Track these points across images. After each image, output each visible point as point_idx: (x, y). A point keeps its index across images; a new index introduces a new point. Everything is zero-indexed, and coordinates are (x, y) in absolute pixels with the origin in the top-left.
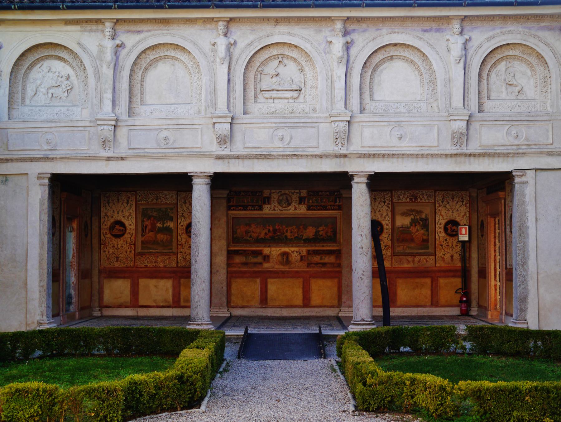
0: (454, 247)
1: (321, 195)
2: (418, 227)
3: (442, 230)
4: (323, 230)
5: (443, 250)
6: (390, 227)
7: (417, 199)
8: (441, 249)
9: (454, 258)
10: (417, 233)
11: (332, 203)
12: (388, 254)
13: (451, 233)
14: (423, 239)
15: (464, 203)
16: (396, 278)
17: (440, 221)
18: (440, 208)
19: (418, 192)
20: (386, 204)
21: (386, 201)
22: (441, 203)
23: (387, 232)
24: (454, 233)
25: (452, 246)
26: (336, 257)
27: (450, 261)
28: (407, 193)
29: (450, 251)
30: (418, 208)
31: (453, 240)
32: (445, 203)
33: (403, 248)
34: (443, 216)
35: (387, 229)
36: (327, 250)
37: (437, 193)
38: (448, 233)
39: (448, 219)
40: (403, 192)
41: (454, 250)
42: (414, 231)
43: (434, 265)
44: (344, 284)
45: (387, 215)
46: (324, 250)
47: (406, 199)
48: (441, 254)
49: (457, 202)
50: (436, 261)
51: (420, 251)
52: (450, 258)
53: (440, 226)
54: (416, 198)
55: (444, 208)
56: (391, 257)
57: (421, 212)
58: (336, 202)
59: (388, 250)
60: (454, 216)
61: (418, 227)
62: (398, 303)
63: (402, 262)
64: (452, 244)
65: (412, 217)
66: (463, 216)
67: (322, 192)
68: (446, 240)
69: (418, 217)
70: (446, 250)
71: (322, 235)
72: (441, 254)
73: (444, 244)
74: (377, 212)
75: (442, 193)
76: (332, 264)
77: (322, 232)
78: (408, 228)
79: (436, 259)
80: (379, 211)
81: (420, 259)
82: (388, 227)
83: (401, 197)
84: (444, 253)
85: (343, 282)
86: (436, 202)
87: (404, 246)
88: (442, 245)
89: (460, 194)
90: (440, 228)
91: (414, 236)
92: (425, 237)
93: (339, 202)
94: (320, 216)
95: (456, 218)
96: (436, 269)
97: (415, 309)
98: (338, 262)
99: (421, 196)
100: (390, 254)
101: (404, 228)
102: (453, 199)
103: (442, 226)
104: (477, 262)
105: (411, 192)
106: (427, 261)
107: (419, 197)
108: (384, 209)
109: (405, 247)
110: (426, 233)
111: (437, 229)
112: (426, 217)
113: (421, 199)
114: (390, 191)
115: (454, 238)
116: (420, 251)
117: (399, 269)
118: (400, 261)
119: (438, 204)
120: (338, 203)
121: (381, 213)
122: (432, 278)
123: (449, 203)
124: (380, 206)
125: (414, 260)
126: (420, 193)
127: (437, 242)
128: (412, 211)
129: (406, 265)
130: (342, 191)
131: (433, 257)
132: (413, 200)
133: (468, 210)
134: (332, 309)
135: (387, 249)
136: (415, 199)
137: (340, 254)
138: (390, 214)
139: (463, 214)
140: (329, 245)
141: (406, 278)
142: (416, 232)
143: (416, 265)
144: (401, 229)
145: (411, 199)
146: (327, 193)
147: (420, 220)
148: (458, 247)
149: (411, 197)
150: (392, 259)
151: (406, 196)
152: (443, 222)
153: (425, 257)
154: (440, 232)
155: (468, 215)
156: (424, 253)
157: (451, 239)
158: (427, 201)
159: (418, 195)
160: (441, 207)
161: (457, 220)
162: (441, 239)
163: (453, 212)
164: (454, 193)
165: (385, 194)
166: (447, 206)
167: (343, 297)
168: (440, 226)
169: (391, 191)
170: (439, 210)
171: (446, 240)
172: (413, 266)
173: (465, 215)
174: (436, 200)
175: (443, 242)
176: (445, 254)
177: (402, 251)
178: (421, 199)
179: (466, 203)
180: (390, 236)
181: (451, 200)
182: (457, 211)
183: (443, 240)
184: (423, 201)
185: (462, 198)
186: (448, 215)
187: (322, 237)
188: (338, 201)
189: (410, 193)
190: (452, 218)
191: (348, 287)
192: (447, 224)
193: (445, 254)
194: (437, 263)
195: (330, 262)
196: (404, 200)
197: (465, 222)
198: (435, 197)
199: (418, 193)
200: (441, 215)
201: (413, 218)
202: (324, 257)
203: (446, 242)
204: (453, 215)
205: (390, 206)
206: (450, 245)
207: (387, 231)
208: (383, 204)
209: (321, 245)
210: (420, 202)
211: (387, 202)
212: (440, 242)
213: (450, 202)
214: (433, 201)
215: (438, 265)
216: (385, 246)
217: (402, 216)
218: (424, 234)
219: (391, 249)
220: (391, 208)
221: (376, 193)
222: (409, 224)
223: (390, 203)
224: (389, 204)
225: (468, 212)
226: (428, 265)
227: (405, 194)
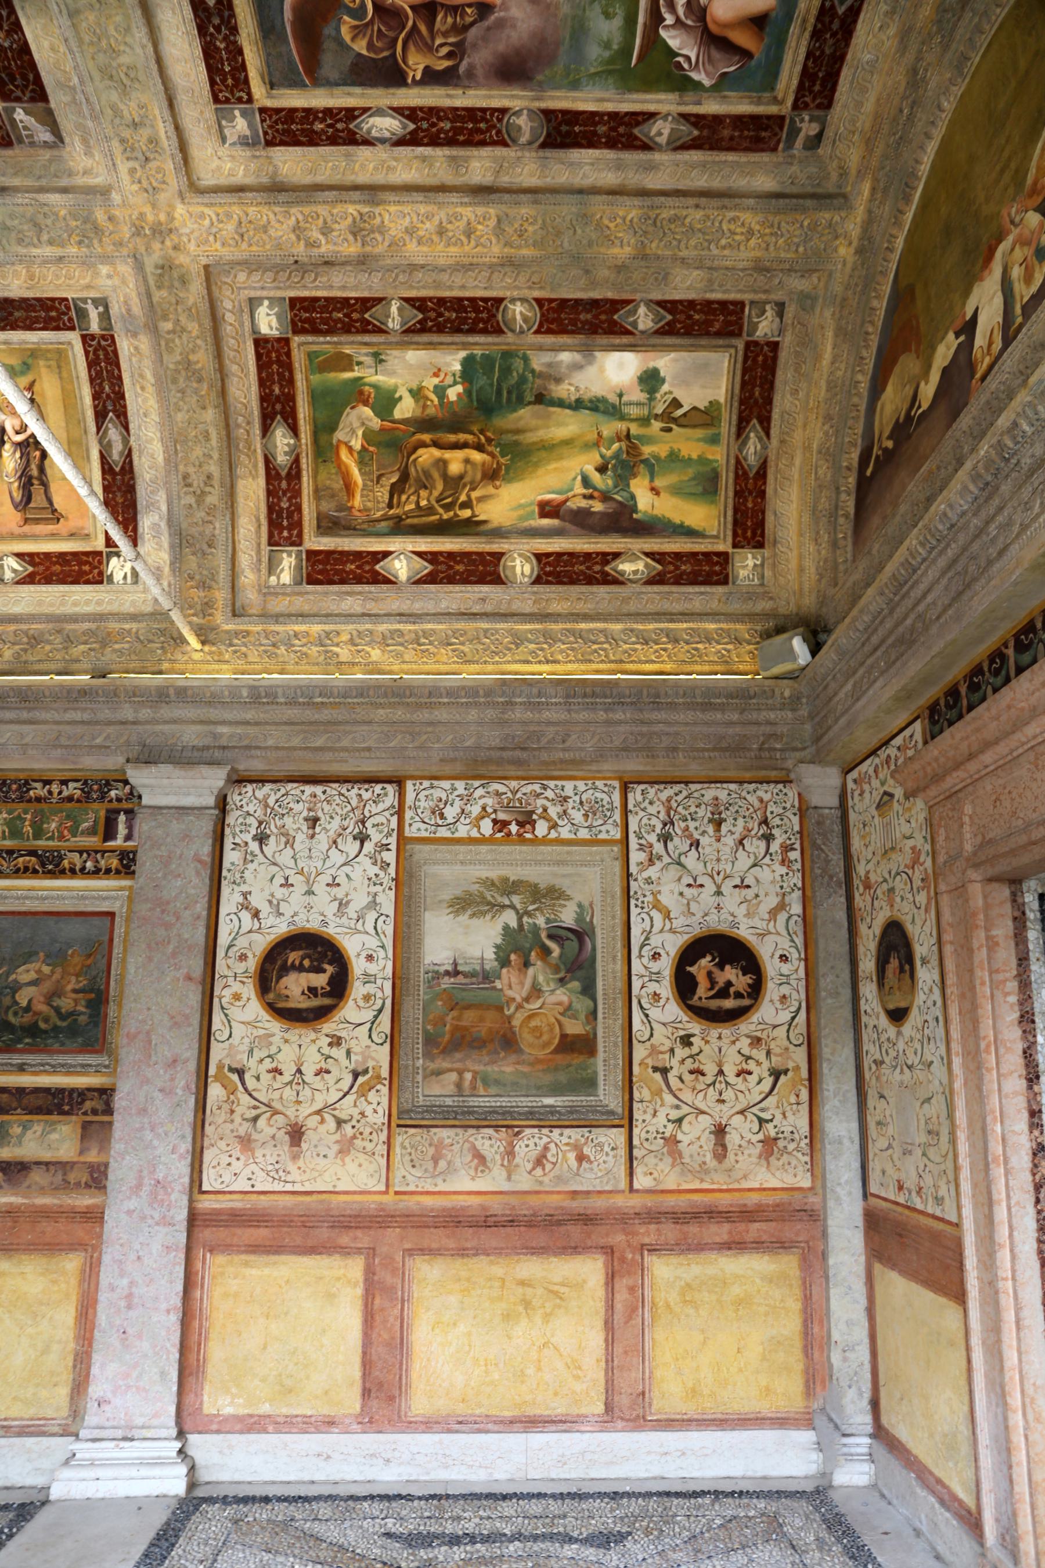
0: (732, 1079)
1: (38, 799)
2: (538, 971)
3: (666, 988)
4: (34, 983)
5: (669, 1098)
6: (384, 967)
7: (533, 823)
8: (658, 1093)
9: (732, 1139)
10: (538, 1004)
11: (93, 841)
12: (372, 1118)
13: (714, 1004)
14: (564, 1036)
15: (775, 847)
16: (410, 1252)
17: (655, 941)
18: (652, 872)
19: (537, 787)
20: (369, 846)
21: (371, 831)
22: (658, 848)
23: (367, 998)
24: (729, 1004)
25: (721, 1072)
26: (86, 1126)
27: (709, 1157)
28: (480, 792)
29: (706, 1101)
30: (538, 875)
31: (725, 1043)
32: (679, 844)
33: (459, 1085)
34: (667, 915)
35: (369, 978)
36: (37, 1090)
37: (635, 796)
38: (694, 1001)
39: (696, 931)
40: (460, 785)
41: (728, 1095)
42: (517, 994)
43: (623, 1185)
44: (112, 1288)
45: (373, 904)
46: (21, 1091)
47: (476, 823)
48: (661, 1119)
49: (741, 842)
50: (631, 1158)
51: (549, 1101)
52: (708, 1142)
53: (655, 966)
54: (527, 820)
55: (674, 871)
56: (383, 1136)
57: (554, 894)
58: (110, 833)
59: (372, 1096)
60: (724, 915)
61: (538, 971)
62: (419, 1404)
63: (442, 1164)
64: (720, 1065)
65: (510, 918)
66: (774, 913)
67: (47, 782)
68: (686, 1041)
69: (541, 921)
70: (687, 1096)
71: (28, 1009)
72: (661, 1119)
73: (675, 1062)
74: (319, 888)
75: (664, 796)
76: (64, 1166)
77: (31, 991)
78: (487, 977)
79: (631, 1146)
80: (334, 884)
81: (546, 1148)
82: (372, 968)
83: (450, 813)
84: (675, 1114)
85: (107, 1275)
86: (632, 837)
87: (461, 1073)
88: (664, 1071)
89: (752, 799)
90: (655, 977)
91: (516, 1022)
92: (575, 1028)
93: (128, 837)
94: (29, 906)
95: (735, 925)
96: (635, 1202)
97: (515, 1441)
98: (92, 1156)
99: (553, 811)
100: (380, 1119)
101: (466, 975)
102: (718, 824)
103: (666, 966)
104: (856, 1165)
105: (502, 789)
106: (581, 1158)
107: (545, 815)
108: (357, 873)
109: (468, 1076)
110: (582, 1005)
111: (636, 984)
112: (580, 918)
113: (554, 826)
114: (390, 782)
115: (726, 1031)
116: (549, 1101)
117: (428, 1201)
118: (435, 1160)
119: (641, 847)
120: (119, 842)
121: (339, 892)
122: (609, 1251)
123: (696, 844)
124: (336, 858)
125: (510, 1153)
126: (549, 794)
127: (639, 1053)
128: (510, 887)
129: (463, 1182)
130: (138, 777)
131: (618, 1136)
132: (514, 828)
133: (797, 880)
134: (30, 1442)
135: (363, 1093)
136: (518, 823)
137: (109, 1111)
138: (387, 902)
139: (773, 901)
140: (61, 1059)
141: (462, 1252)
142: (527, 1000)
143: (523, 1182)
144: (446, 982)
145: (500, 825)
146: (73, 789)
147: (550, 937)
148: (753, 1079)
149: (502, 816)
150: (389, 1143)
151: (476, 810)
152: (672, 945)
153: (575, 1134)
154: (656, 996)
155: (797, 909)
156: (572, 1110)
157: (714, 1033)
158: (584, 834)
159: (540, 802)
160: (659, 865)
161: (744, 932)
162: (662, 1038)
163: (719, 893)
164: (723, 795)
165: (366, 795)
166: (691, 861)
167: (95, 1370)
168: (655, 966)
169: (399, 782)
170: (649, 881)
171: (686, 1041)
172: (506, 1187)
173: (782, 906)
174: (633, 827)
175: (672, 1051)
176: (679, 1121)
177: (449, 1101)
178: (554, 826)
179: (787, 848)
180: (386, 1018)
181: (711, 829)
182: (742, 886)
183: (668, 1044)
184: (565, 833)
185: (765, 822)
186: (694, 907)
187: (27, 1019)
188: (122, 830)
189: (498, 794)
190: (717, 923)
191: (129, 1307)
192: (690, 953)
193: (679, 1121)
194: (639, 1170)
195: (47, 1156)
196: (462, 831)
197: (785, 944)
198: (625, 812)
199: (538, 795)
200: (657, 905)
201: (513, 924)
202: (17, 1130)
203: (687, 1052)
204: (718, 908)
205: (390, 857)
206: (710, 1069)
207: (370, 988)
208: (353, 847)
209: (17, 1059)
210: (545, 841)
211: (375, 836)
212: (654, 1051)
213: (704, 841)
214: (617, 834)
215: (642, 1181)
216: (356, 1075)
217: (457, 913)
218: (568, 1010)
219: (385, 1090)
220: (392, 870)
221: (318, 789)
222: (490, 954)
223: (393, 840)
224: (386, 847)
225: (798, 894)
226: (589, 1180)
227: (468, 799)
